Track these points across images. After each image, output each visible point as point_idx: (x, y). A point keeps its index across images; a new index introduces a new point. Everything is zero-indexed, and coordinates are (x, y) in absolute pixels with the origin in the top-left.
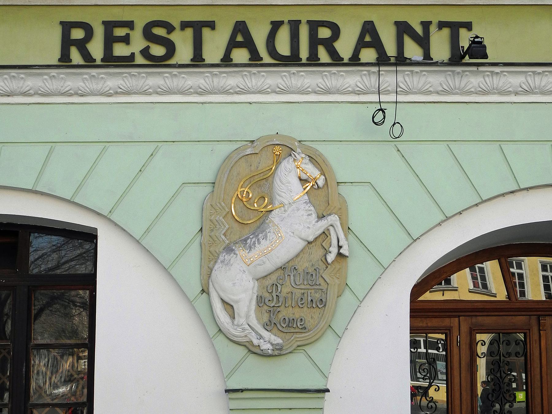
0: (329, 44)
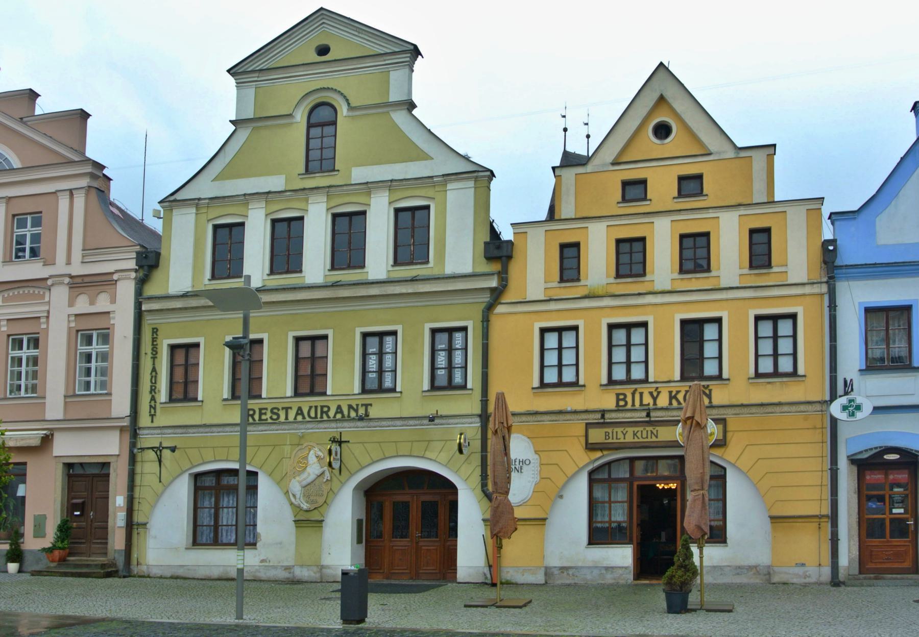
0: (327, 413)
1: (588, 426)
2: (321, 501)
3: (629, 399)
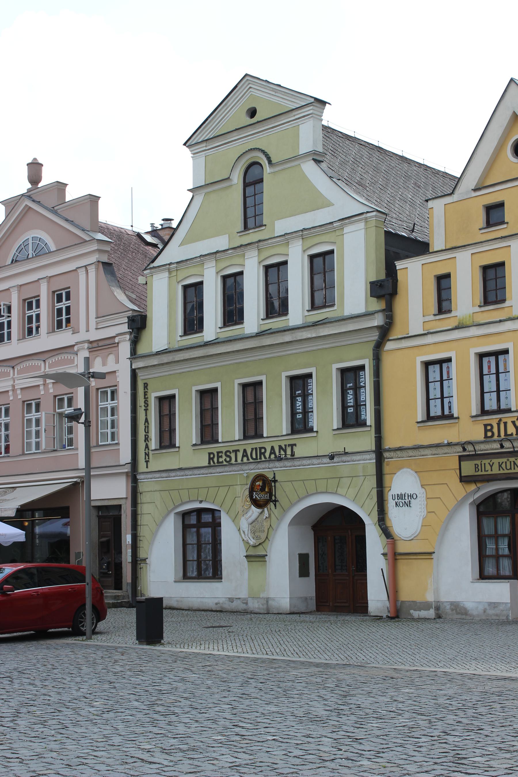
0: (264, 454)
1: (461, 458)
2: (263, 536)
3: (495, 430)
